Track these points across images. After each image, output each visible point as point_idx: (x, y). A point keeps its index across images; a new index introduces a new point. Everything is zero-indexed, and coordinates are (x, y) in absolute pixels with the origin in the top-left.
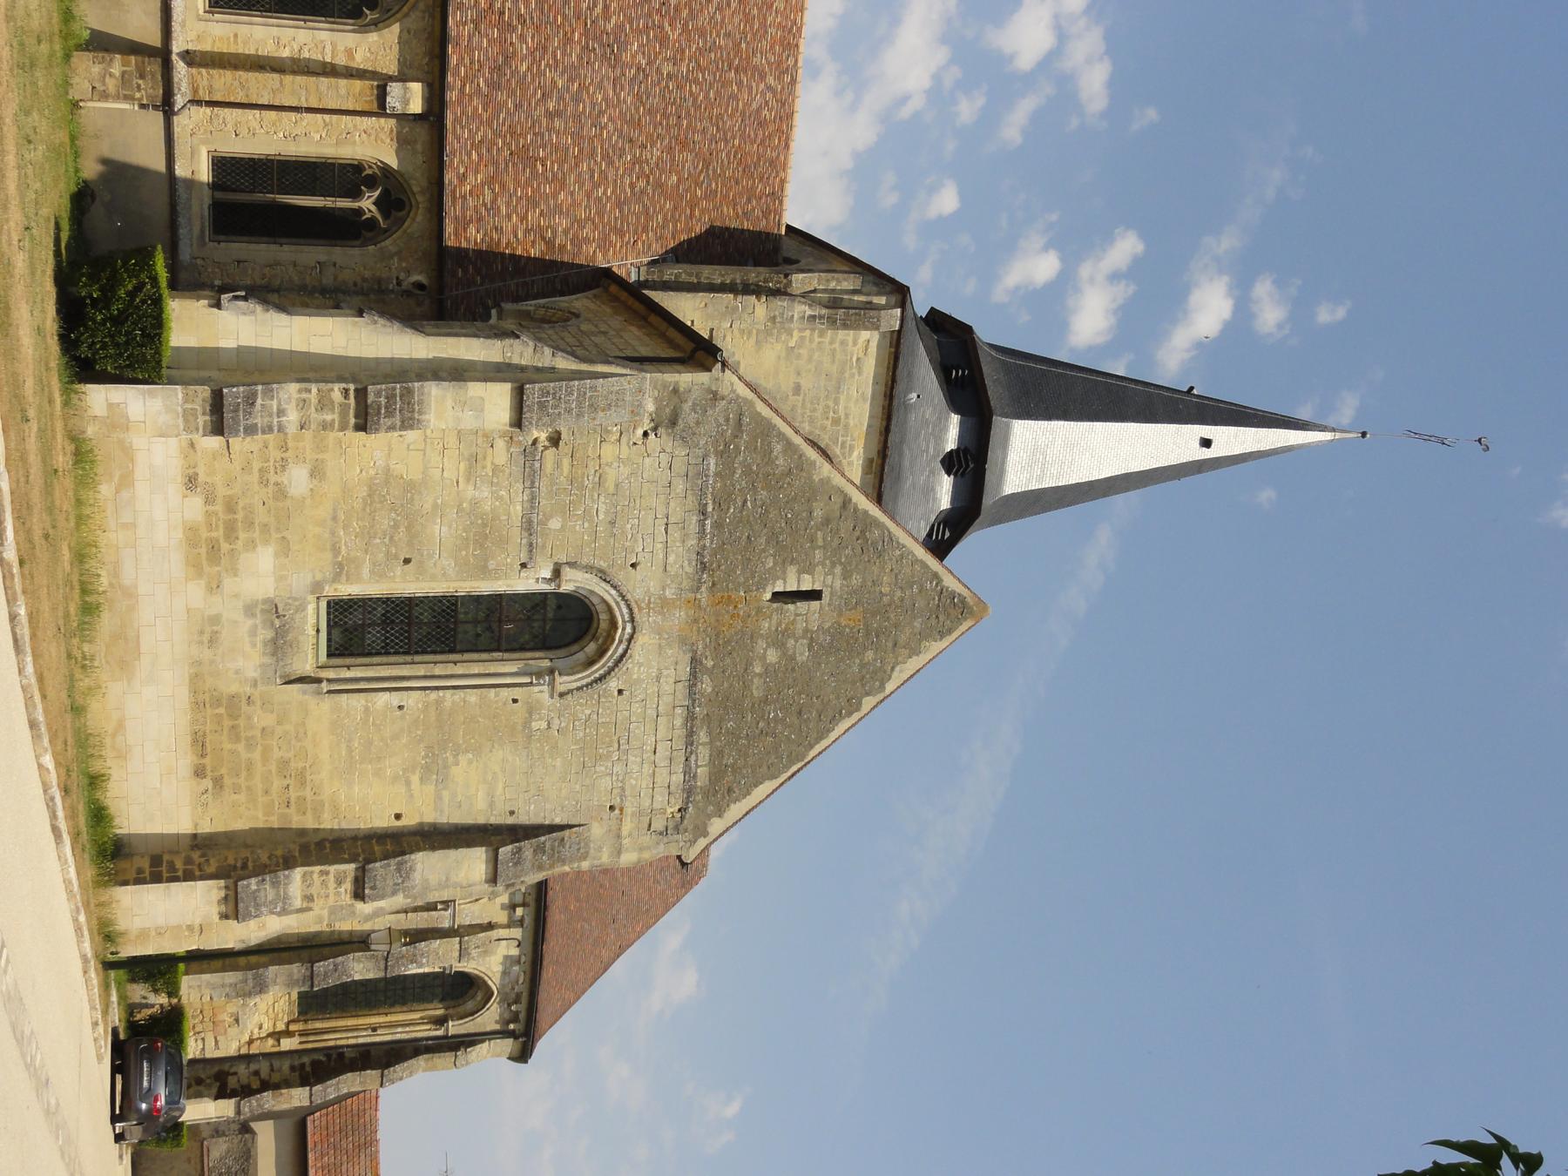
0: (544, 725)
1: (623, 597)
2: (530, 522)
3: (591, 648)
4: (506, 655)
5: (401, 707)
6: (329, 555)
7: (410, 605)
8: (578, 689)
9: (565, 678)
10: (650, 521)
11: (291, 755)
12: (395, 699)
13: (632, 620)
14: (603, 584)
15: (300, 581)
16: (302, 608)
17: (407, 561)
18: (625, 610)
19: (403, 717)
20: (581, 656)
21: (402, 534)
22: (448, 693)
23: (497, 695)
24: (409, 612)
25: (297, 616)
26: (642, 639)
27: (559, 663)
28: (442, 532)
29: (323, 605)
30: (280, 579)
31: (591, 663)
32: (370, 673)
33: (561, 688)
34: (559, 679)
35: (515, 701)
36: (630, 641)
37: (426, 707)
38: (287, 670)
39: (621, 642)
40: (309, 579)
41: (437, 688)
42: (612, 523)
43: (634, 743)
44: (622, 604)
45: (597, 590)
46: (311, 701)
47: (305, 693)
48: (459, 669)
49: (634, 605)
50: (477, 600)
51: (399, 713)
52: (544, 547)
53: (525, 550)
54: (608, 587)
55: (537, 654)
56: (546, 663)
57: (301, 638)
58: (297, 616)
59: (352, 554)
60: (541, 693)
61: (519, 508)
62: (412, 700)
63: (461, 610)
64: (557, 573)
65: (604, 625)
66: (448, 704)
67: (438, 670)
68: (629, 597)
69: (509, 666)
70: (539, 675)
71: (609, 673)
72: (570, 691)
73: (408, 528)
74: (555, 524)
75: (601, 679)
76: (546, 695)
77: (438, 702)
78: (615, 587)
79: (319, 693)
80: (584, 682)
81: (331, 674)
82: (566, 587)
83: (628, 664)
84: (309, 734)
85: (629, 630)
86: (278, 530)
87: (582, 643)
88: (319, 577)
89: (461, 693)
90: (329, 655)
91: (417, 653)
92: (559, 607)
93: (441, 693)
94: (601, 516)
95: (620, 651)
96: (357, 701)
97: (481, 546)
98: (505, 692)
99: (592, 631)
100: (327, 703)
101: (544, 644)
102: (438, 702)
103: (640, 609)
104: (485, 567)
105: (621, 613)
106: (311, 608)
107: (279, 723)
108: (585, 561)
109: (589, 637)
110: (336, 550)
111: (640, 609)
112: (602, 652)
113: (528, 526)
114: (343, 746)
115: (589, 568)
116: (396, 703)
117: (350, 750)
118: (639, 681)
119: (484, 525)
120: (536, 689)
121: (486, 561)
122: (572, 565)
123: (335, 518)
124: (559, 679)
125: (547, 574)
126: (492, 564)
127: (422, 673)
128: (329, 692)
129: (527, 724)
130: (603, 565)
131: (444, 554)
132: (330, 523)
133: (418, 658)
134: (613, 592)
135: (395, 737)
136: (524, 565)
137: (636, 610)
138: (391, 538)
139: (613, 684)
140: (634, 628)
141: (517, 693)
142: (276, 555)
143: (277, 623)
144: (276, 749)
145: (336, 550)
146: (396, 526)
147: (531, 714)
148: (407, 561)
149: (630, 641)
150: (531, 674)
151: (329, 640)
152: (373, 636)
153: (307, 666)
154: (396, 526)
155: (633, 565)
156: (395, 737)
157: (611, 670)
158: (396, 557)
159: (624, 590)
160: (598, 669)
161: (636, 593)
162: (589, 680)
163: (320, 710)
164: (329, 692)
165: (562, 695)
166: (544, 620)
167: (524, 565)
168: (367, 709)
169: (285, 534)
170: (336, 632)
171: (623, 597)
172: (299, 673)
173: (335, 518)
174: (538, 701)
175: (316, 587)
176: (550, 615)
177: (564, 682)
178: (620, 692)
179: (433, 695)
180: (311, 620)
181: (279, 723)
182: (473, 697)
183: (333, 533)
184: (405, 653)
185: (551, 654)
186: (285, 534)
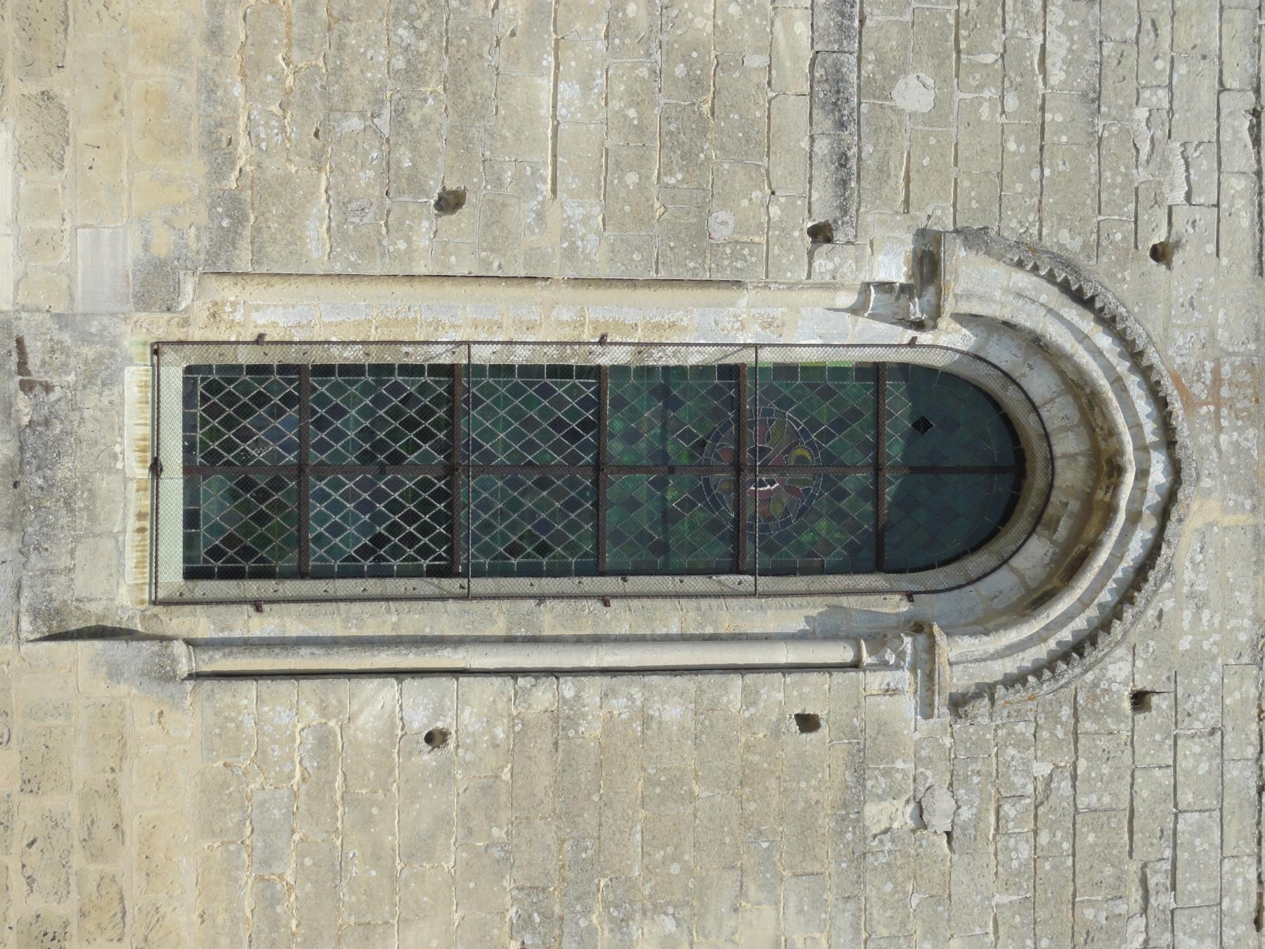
0: (903, 816)
1: (1134, 355)
2: (837, 80)
3: (1035, 554)
4: (765, 583)
5: (434, 738)
6: (194, 167)
7: (449, 400)
8: (1015, 681)
9: (968, 645)
10: (1206, 98)
11: (67, 909)
12: (418, 706)
13: (1169, 440)
14: (1072, 312)
15: (101, 255)
16: (102, 374)
17: (450, 202)
18: (1144, 407)
19: (443, 775)
20: (1003, 581)
21: (431, 101)
22: (593, 687)
23: (750, 699)
24: (449, 423)
25: (91, 401)
26: (1208, 513)
27: (929, 606)
28: (560, 98)
29: (173, 379)
30: (34, 245)
31: (1039, 599)
32: (329, 622)
33: (955, 680)
34: (952, 649)
35: (807, 723)
36: (1164, 514)
37: (521, 733)
38: (57, 588)
39: (1134, 518)
40: (132, 251)
41: (579, 640)
42: (1093, 99)
43: (1188, 884)
44: (1133, 383)
45: (1055, 333)
46: (139, 703)
47: (115, 673)
48: (620, 619)
49: (1169, 389)
50: (665, 384)
51: (429, 758)
52: (883, 171)
53: (824, 175)
54: (1087, 324)
55: (863, 581)
56: (896, 606)
57: (104, 484)
58: (91, 401)
59: (273, 167)
60: (889, 694)
61: (802, 28)
62: (474, 710)
63: (615, 424)
64: (928, 265)
65: (1070, 476)
66: (591, 729)
67: (550, 619)
68: (1152, 357)
69: (775, 616)
70: (879, 637)
71: (1105, 626)
72: (986, 690)
73: (455, 82)
74: (914, 95)
75: (1078, 648)
76: (908, 704)
77: (562, 721)
78: (1108, 322)
79: (167, 677)
80: (1027, 658)
81: (202, 624)
82: (948, 342)
83: (1161, 597)
84: (133, 828)
85: (1158, 475)
86: (28, 67)
87: (1003, 544)
88: (163, 243)
89: (634, 689)
90: (191, 574)
91: (479, 573)
92: (921, 425)
93: (568, 687)
94: (1057, 76)
95: (1136, 549)
96: (290, 712)
97: (689, 156)
98: (774, 691)
99: (1031, 502)
100: (192, 714)
101: (877, 555)
102: (562, 721)
103: (1190, 403)
104: (702, 232)
105: (1132, 416)
106: (135, 377)
107: (29, 785)
108: (1012, 227)
109: (1021, 523)
110: (219, 152)
111: (1190, 403)
112: (1071, 565)
113: (834, 96)
114: (247, 878)
115: (1026, 256)
116: (420, 722)
117: (269, 899)
118: (1199, 660)
119: (695, 84)
120: (875, 681)
121: (703, 210)
122: (975, 238)
123: (214, 36)
124: (952, 649)
125: (893, 267)
126: (722, 224)
127: (499, 628)
128: (196, 676)
129: (849, 809)
130: (1067, 240)
131: (569, 182)
132: (198, 48)
133: (480, 585)
134: (1104, 341)
135: (420, 849)
136: (821, 234)
137: (1177, 406)
138: (400, 114)
139: (1118, 670)
140: (1175, 469)
141: (812, 694)
142: (23, 158)
143: (23, 404)
144: (17, 883)
145: (219, 152)
146: (413, 73)
147: (861, 780)
148: (450, 202)
149: (1164, 514)
150: (853, 639)
151: (191, 519)
152: (337, 510)
153: (123, 597)
154: (413, 73)
155: (1160, 254)
156: (420, 849)
157: (1113, 614)
158: (415, 183)
159: (1137, 332)
160: (1069, 612)
161: (1174, 352)
162: (1040, 652)
163: (168, 746)
164: (196, 676)
165: (958, 704)
166: (877, 468)
167: (821, 234)
168: (324, 741)
169: (54, 83)
170: (214, 490)
171: (1134, 355)
172: (95, 612)
173: (214, 36)
174: (882, 726)
175: (155, 285)
176: (894, 450)
177: (968, 657)
178: (1140, 700)
179: (543, 696)
180: (135, 426)
181: (29, 785)
182: (673, 706)
183: (210, 89)
184: (434, 572)
185: (906, 581)
186: (54, 83)
